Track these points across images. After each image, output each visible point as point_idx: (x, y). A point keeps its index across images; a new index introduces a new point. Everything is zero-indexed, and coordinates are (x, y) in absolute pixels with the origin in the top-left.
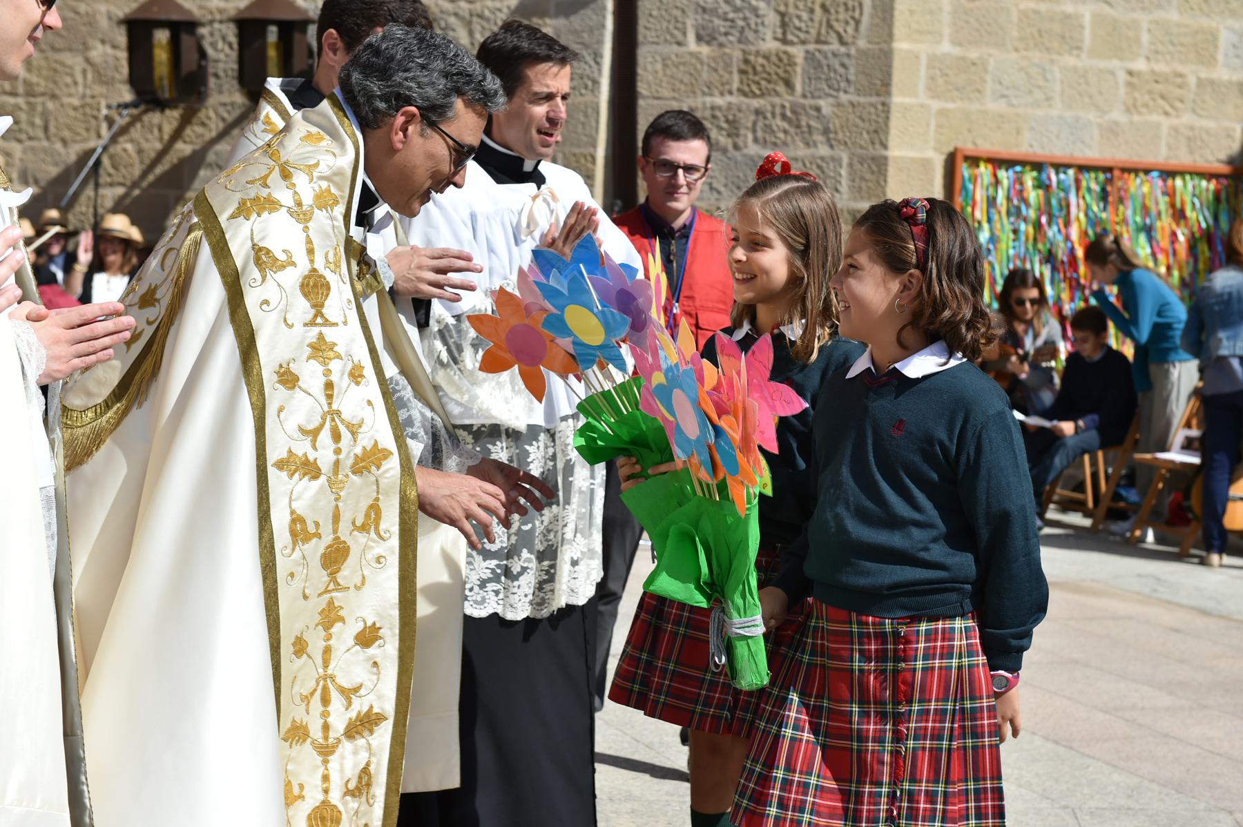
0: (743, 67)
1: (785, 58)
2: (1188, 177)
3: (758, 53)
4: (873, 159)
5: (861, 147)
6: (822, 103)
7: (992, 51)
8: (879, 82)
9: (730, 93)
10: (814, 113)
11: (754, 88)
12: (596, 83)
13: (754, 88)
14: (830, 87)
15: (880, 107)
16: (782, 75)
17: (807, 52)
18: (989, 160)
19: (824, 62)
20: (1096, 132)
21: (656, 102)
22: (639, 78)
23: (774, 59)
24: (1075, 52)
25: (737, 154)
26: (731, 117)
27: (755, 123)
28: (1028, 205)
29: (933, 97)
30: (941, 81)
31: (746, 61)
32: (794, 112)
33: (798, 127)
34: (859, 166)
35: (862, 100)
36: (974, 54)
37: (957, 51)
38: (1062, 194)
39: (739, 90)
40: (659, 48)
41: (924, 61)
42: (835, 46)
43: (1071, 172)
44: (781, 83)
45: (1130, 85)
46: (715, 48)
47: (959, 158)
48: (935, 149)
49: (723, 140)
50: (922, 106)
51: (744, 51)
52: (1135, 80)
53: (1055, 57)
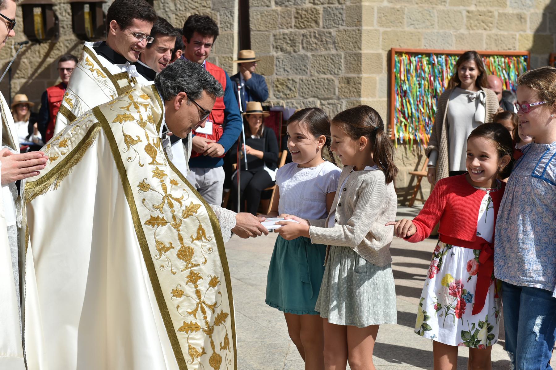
0: (297, 16)
1: (314, 11)
2: (496, 57)
3: (302, 9)
4: (355, 54)
5: (350, 50)
6: (331, 30)
7: (406, 5)
8: (356, 20)
9: (291, 27)
10: (329, 35)
11: (301, 24)
12: (232, 25)
13: (301, 24)
14: (334, 23)
15: (357, 31)
17: (324, 8)
18: (407, 53)
19: (332, 12)
20: (454, 39)
21: (258, 32)
22: (250, 22)
23: (310, 11)
24: (443, 3)
25: (295, 54)
26: (292, 38)
27: (302, 41)
28: (424, 72)
29: (380, 26)
30: (384, 19)
31: (298, 13)
32: (319, 35)
33: (322, 41)
34: (349, 58)
35: (349, 28)
36: (398, 6)
37: (391, 5)
38: (440, 67)
39: (295, 26)
40: (259, 8)
41: (376, 11)
42: (337, 5)
43: (443, 57)
44: (313, 22)
45: (468, 17)
46: (284, 7)
47: (393, 53)
48: (383, 49)
49: (289, 49)
50: (376, 30)
51: (296, 9)
52: (470, 15)
53: (434, 6)
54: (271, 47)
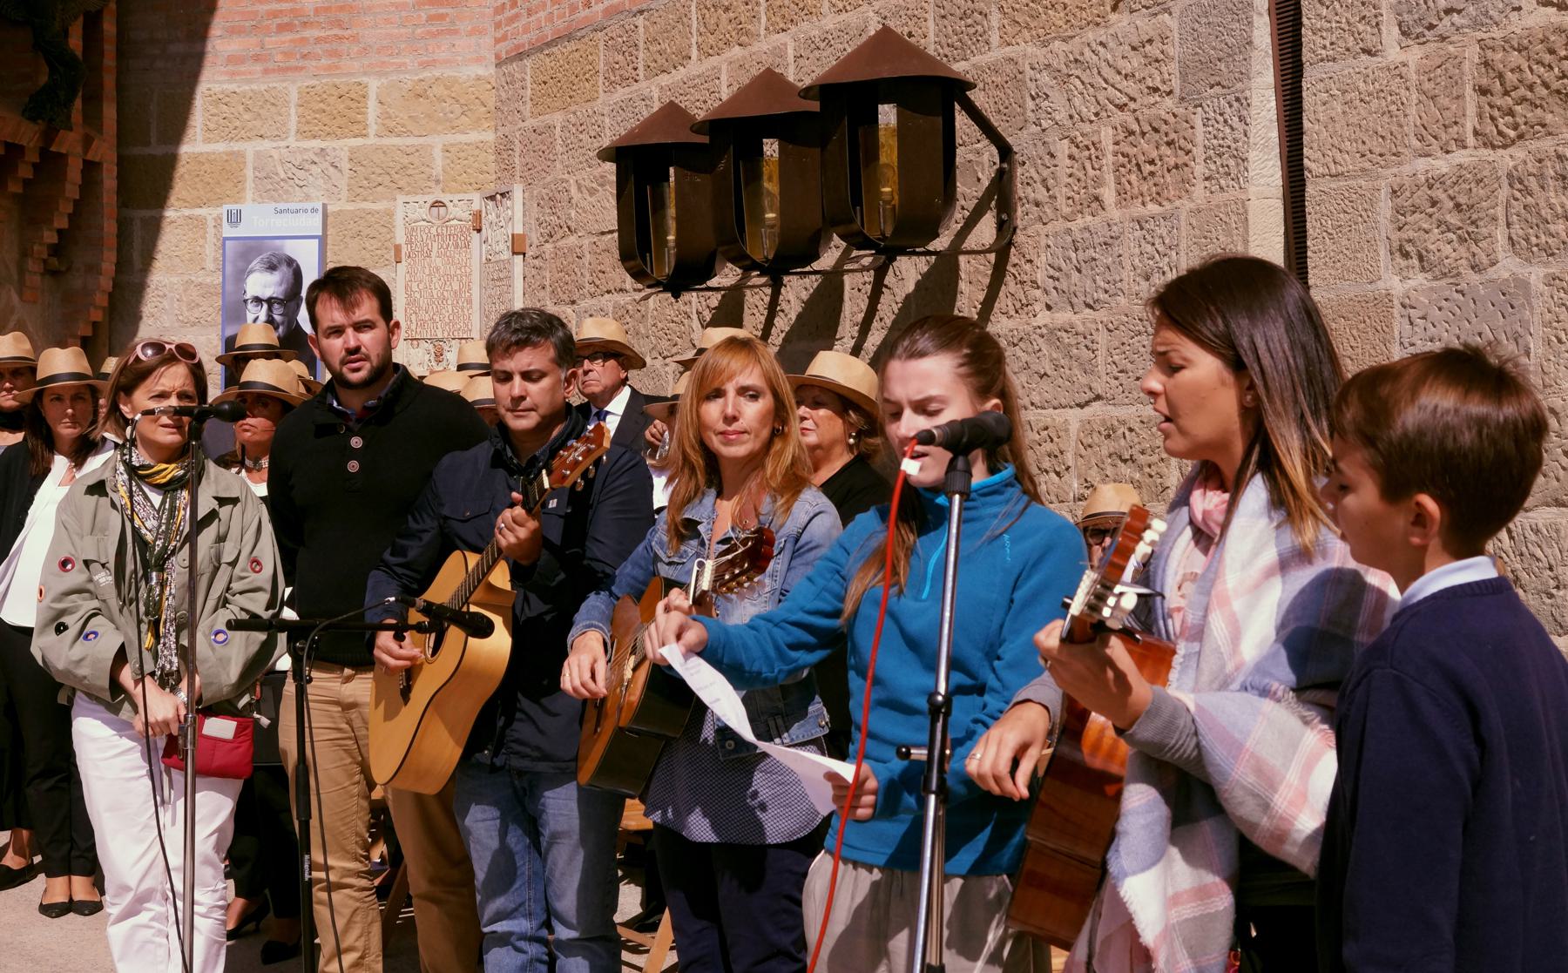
0: (1484, 82)
16: (1556, 85)
25: (1474, 278)
26: (1462, 199)
54: (1383, 252)
